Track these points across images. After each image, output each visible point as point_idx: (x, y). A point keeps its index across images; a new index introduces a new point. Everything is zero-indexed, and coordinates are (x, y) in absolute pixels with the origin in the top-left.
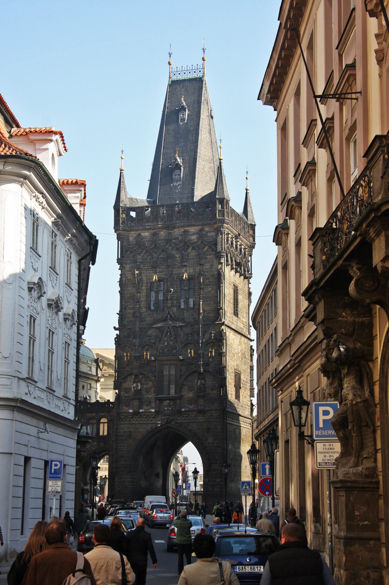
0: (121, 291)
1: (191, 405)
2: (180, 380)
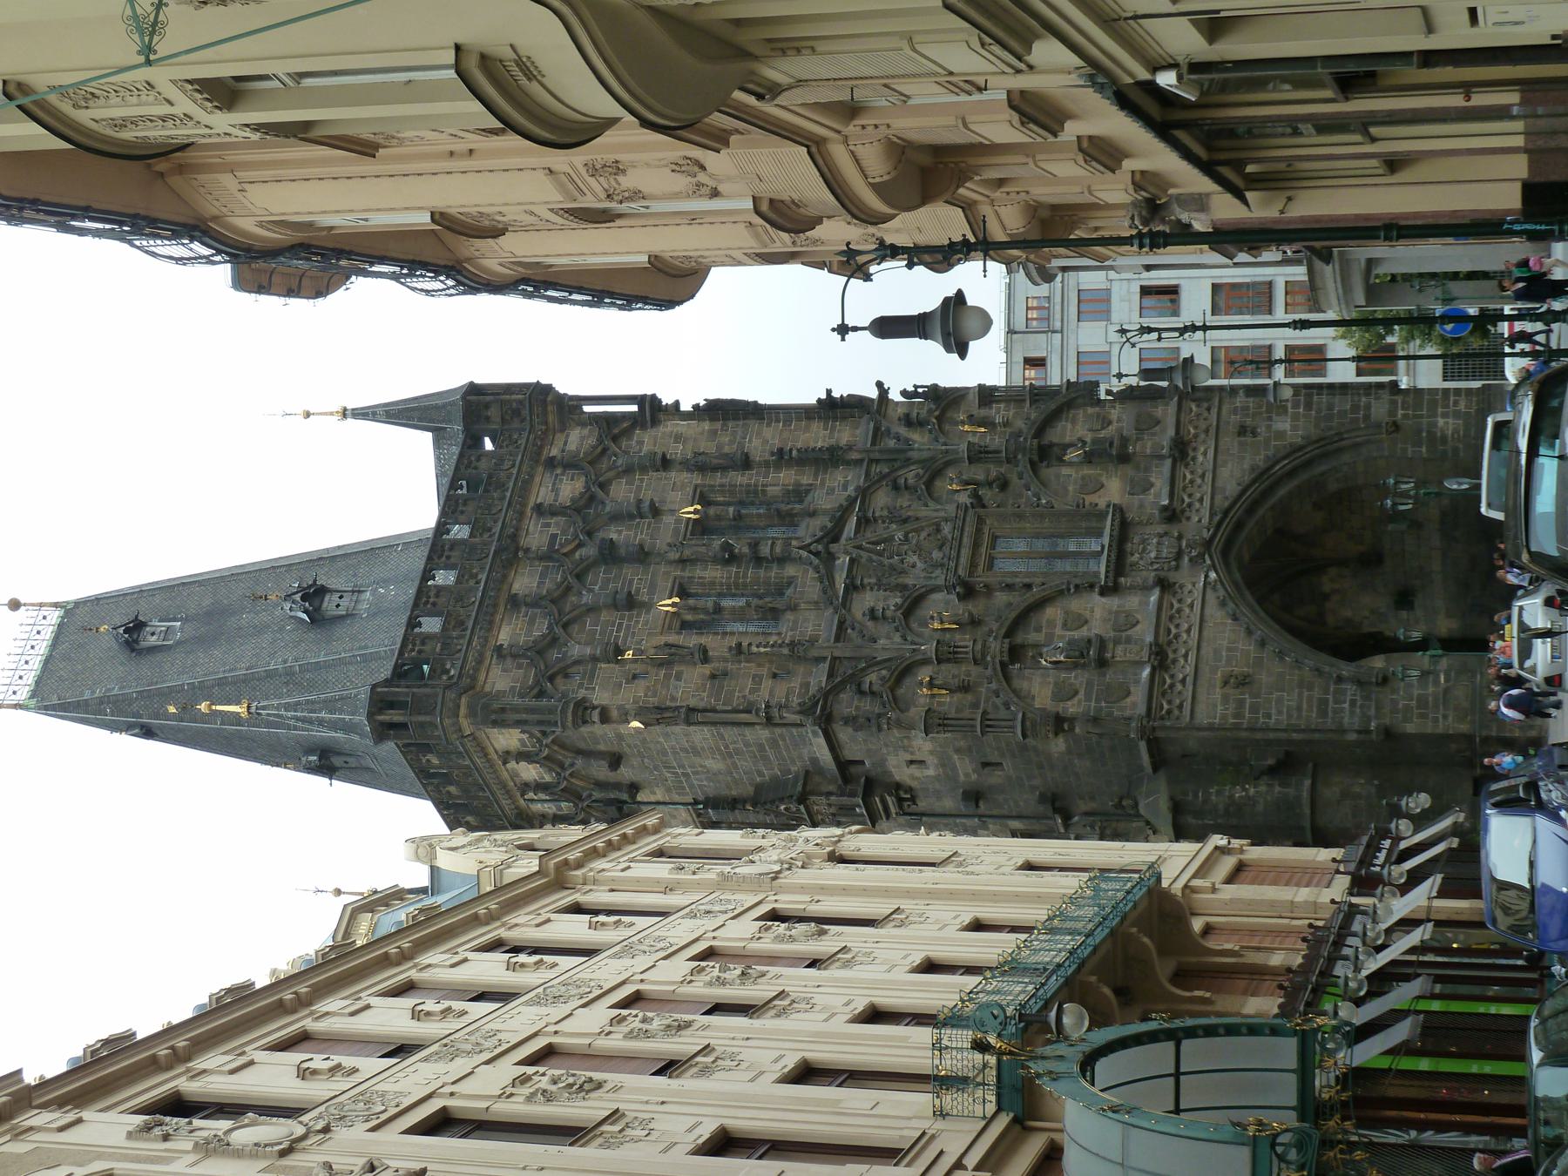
1: (1152, 485)
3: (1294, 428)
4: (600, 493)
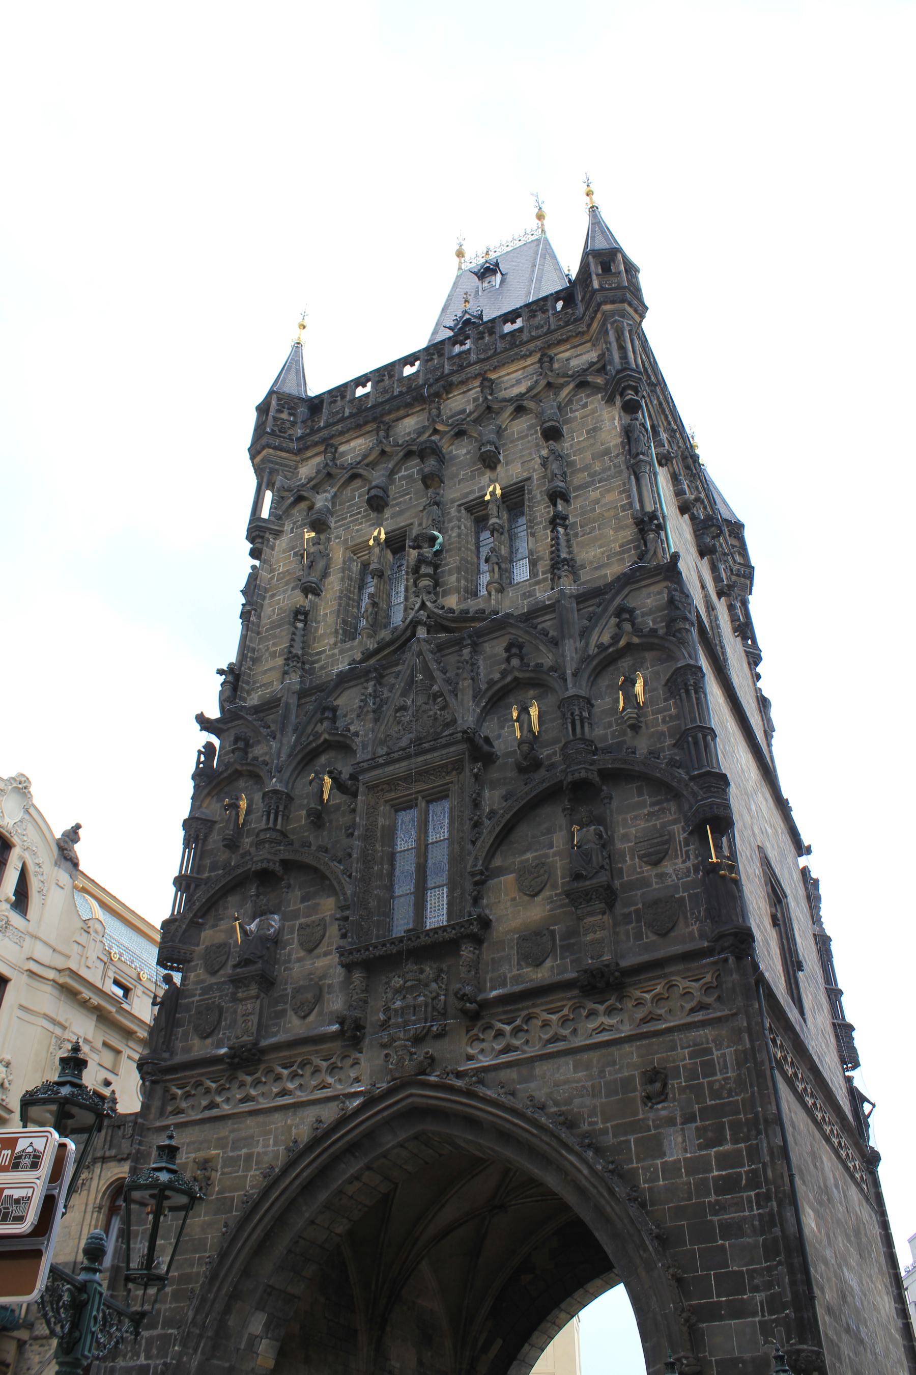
0: (248, 608)
1: (538, 964)
2: (474, 843)
3: (671, 1170)
4: (510, 409)
